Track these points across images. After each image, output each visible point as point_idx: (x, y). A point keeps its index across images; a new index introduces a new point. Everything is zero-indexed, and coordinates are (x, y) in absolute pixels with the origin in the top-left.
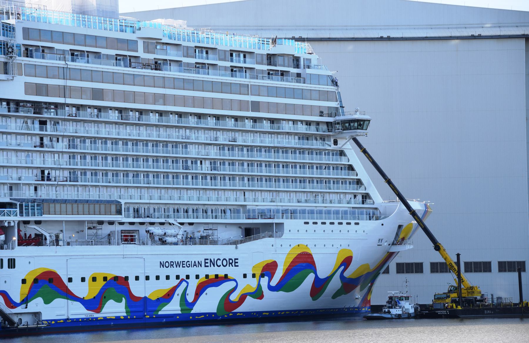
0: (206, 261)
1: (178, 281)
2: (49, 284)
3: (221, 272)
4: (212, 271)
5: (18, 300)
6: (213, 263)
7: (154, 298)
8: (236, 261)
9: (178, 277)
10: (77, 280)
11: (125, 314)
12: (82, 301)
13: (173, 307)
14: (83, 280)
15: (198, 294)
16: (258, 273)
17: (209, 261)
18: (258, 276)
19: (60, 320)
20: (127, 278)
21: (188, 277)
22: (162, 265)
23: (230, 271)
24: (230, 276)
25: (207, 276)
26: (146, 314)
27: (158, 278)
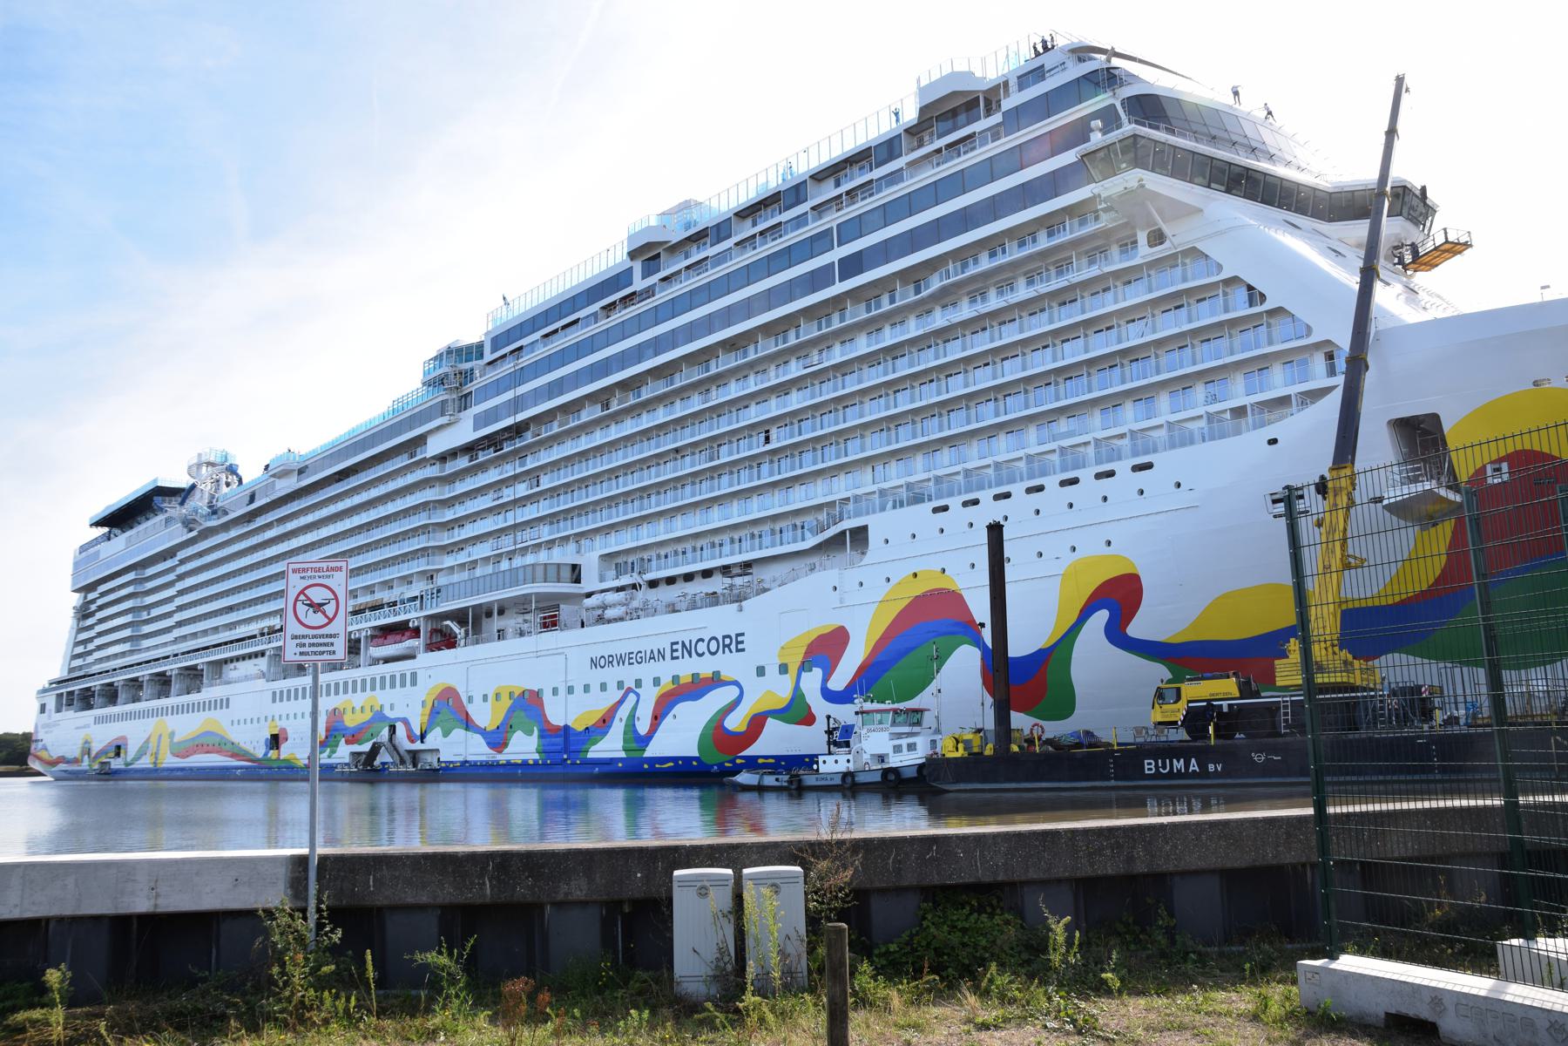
3: (704, 666)
4: (687, 668)
6: (688, 650)
9: (620, 685)
10: (478, 699)
11: (537, 756)
12: (482, 732)
13: (610, 747)
14: (485, 698)
15: (657, 718)
16: (794, 662)
17: (679, 647)
18: (793, 669)
21: (638, 683)
22: (594, 663)
23: (726, 664)
24: (725, 675)
25: (675, 678)
27: (587, 688)
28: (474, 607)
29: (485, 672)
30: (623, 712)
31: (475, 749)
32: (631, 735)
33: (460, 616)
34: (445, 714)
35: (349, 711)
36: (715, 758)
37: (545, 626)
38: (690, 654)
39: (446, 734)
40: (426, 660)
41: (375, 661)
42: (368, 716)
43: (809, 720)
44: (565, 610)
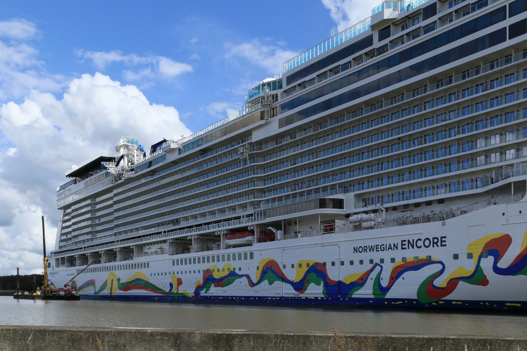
0: (404, 243)
1: (372, 265)
2: (271, 271)
3: (422, 254)
4: (411, 254)
5: (255, 282)
6: (411, 244)
7: (348, 282)
8: (443, 239)
9: (371, 261)
10: (289, 266)
11: (323, 296)
13: (366, 292)
14: (293, 266)
17: (406, 243)
19: (277, 297)
20: (325, 264)
21: (382, 261)
22: (356, 250)
24: (434, 258)
25: (404, 259)
26: (339, 296)
27: (352, 263)
28: (285, 220)
29: (293, 253)
30: (373, 275)
31: (288, 291)
32: (377, 287)
33: (277, 225)
34: (270, 273)
35: (216, 271)
36: (426, 300)
37: (326, 230)
38: (413, 247)
39: (271, 283)
40: (257, 246)
41: (228, 247)
42: (226, 273)
43: (485, 282)
44: (338, 223)
